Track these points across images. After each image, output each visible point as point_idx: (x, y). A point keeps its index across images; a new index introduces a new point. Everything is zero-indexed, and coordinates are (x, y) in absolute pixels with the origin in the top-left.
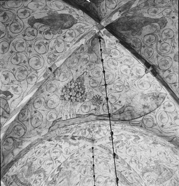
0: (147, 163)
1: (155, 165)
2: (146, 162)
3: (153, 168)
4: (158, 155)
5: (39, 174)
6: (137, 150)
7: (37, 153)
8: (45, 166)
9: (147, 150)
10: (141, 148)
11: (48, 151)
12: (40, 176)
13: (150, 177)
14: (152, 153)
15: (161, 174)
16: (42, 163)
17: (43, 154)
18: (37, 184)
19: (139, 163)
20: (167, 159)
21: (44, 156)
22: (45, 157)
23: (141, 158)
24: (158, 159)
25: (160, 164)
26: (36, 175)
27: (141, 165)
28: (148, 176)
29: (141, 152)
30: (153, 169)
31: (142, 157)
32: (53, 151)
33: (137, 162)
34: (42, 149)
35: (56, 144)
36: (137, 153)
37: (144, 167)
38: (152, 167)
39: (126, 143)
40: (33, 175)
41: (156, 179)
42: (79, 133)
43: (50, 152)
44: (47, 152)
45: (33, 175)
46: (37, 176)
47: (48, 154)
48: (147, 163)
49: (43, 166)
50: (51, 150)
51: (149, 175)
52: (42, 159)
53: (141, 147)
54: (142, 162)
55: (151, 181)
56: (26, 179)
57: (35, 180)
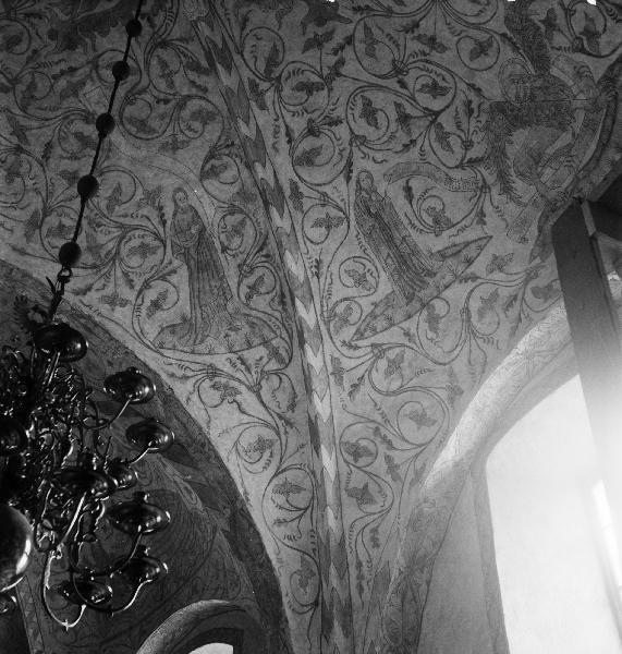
5: (543, 28)
7: (436, 105)
8: (490, 14)
11: (409, 36)
12: (550, 23)
16: (482, 37)
17: (436, 56)
18: (600, 29)
21: (444, 49)
22: (445, 36)
26: (553, 54)
32: (397, 8)
34: (411, 85)
35: (358, 17)
40: (554, 71)
42: (181, 40)
43: (406, 21)
44: (419, 38)
45: (554, 71)
46: (560, 40)
47: (426, 27)
49: (492, 25)
50: (398, 22)
52: (467, 46)
56: (580, 116)
57: (582, 50)
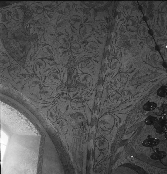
0: (38, 21)
1: (31, 32)
2: (40, 21)
3: (26, 28)
4: (46, 44)
6: (61, 15)
9: (55, 28)
10: (60, 21)
13: (15, 18)
14: (49, 36)
15: (15, 38)
19: (44, 10)
20: (41, 59)
23: (48, 16)
24: (39, 41)
25: (32, 43)
27: (39, 11)
28: (17, 15)
29: (56, 20)
30: (25, 27)
31: (49, 19)
33: (47, 8)
36: (58, 14)
37: (35, 15)
38: (28, 26)
39: (80, 7)
41: (8, 27)
48: (38, 21)
51: (17, 18)
53: (62, 23)
54: (43, 15)
55: (7, 17)
